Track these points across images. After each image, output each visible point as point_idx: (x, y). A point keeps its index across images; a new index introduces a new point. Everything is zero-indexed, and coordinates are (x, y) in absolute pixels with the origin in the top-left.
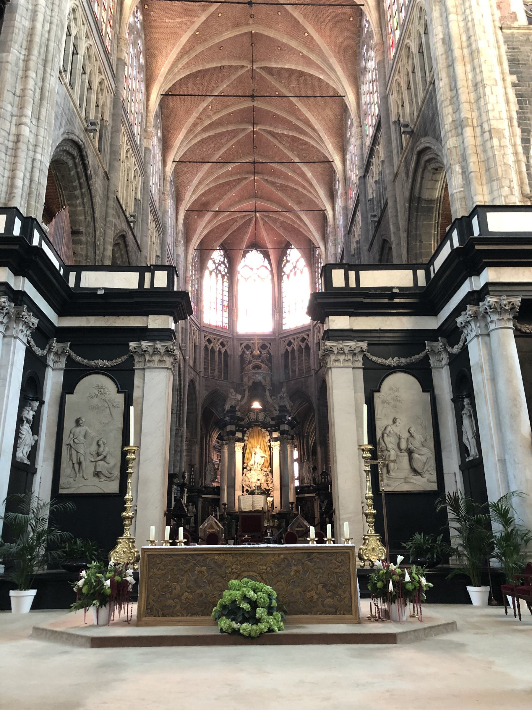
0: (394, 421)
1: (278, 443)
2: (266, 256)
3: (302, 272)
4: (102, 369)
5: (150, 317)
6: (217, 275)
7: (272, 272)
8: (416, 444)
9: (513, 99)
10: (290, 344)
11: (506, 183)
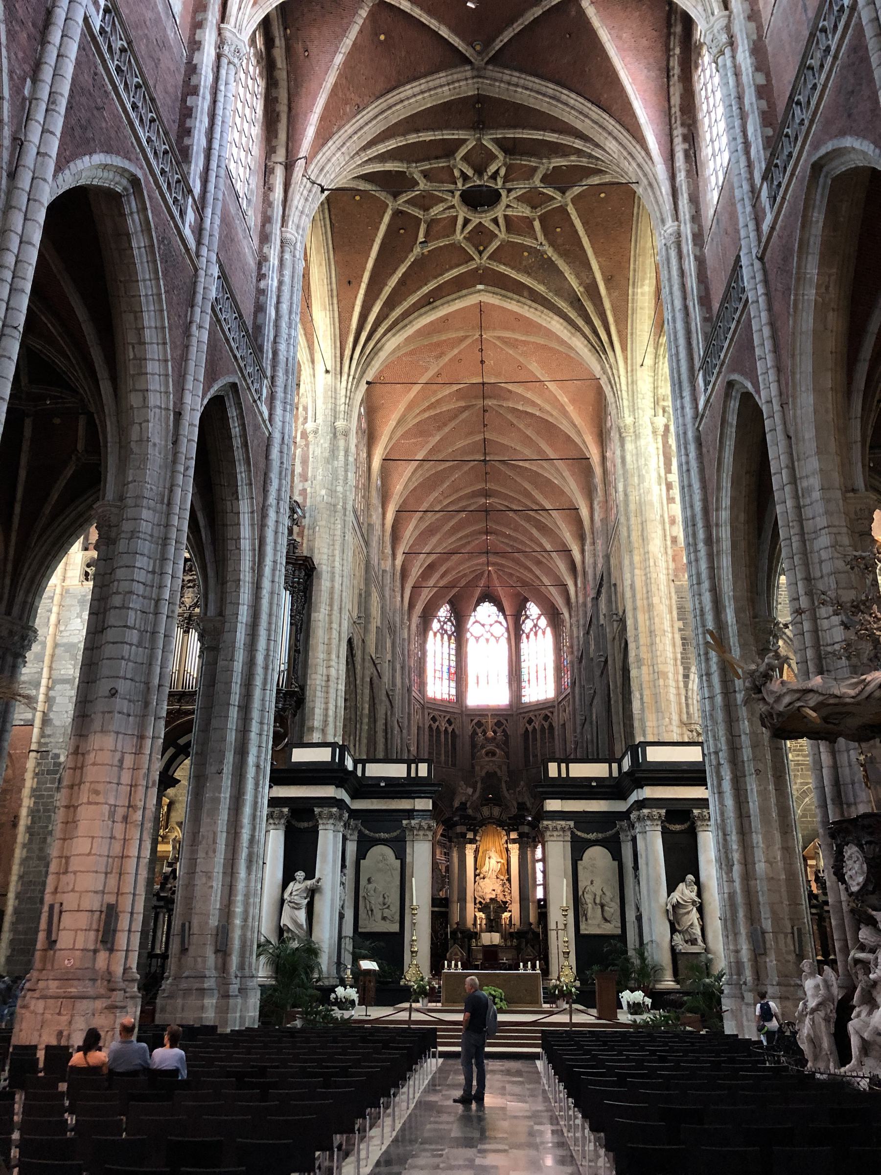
0: (592, 883)
1: (517, 846)
2: (501, 609)
3: (544, 633)
4: (384, 840)
5: (417, 800)
6: (442, 635)
7: (508, 629)
8: (607, 899)
9: (679, 642)
10: (530, 721)
11: (667, 715)
